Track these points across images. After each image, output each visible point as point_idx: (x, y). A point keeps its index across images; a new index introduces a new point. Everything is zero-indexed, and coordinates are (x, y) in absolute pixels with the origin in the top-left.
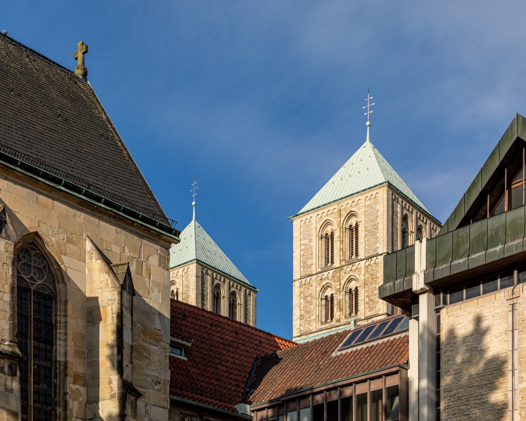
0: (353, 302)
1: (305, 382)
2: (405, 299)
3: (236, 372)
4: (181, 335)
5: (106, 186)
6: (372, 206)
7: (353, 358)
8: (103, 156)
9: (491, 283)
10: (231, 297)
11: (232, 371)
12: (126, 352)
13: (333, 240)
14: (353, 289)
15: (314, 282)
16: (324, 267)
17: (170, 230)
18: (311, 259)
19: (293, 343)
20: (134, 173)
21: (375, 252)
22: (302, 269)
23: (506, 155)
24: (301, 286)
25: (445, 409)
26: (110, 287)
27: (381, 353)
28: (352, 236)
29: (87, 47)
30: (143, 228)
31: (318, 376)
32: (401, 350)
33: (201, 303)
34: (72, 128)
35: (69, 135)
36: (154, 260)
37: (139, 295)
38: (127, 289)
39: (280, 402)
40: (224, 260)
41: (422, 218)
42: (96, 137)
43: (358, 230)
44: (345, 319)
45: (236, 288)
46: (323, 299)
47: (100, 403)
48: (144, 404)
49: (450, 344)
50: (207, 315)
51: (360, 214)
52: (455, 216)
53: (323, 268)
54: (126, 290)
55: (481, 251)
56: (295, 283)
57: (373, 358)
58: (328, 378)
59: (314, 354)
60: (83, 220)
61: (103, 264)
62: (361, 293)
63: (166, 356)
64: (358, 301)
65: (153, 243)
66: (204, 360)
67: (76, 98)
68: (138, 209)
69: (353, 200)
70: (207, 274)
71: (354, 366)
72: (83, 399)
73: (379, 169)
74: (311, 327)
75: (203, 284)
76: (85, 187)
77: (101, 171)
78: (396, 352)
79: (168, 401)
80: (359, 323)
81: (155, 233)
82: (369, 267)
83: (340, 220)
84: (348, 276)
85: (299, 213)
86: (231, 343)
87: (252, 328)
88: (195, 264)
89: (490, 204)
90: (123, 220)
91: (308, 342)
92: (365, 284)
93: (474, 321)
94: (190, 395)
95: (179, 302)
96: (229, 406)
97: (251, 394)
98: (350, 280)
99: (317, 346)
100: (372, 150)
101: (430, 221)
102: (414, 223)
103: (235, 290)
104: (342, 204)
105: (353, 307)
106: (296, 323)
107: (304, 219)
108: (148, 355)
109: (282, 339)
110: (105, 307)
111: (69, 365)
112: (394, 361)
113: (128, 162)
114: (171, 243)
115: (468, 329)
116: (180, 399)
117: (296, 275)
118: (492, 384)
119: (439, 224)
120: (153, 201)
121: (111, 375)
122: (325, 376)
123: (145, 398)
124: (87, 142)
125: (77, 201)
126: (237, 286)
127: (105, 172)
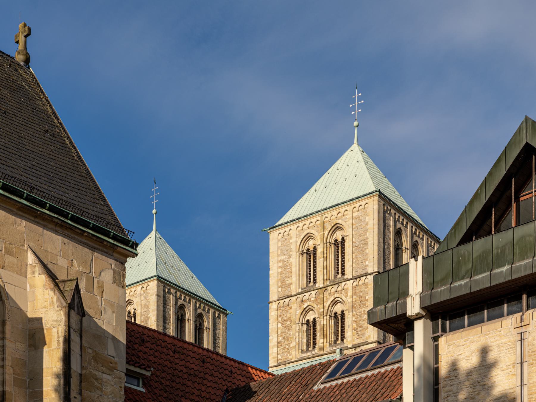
0: (338, 328)
2: (398, 325)
4: (139, 363)
5: (51, 189)
6: (361, 218)
7: (338, 392)
8: (48, 155)
9: (497, 308)
10: (198, 319)
12: (74, 381)
13: (316, 256)
14: (339, 313)
15: (294, 304)
16: (305, 287)
17: (126, 242)
18: (291, 278)
19: (269, 374)
20: (84, 175)
21: (363, 271)
22: (280, 289)
23: (513, 162)
24: (278, 308)
27: (370, 387)
28: (338, 252)
29: (29, 29)
30: (95, 238)
32: (394, 384)
33: (162, 326)
34: (12, 122)
35: (8, 130)
36: (107, 276)
37: (90, 316)
38: (76, 308)
40: (189, 277)
41: (417, 233)
42: (40, 133)
43: (344, 245)
44: (329, 347)
45: (204, 310)
46: (304, 324)
49: (449, 377)
51: (346, 227)
52: (455, 231)
53: (304, 288)
54: (74, 310)
55: (485, 272)
56: (272, 305)
57: (362, 392)
59: (293, 387)
60: (24, 229)
61: (48, 279)
62: (348, 318)
63: (121, 387)
64: (344, 327)
65: (106, 256)
66: (165, 392)
67: (17, 87)
68: (89, 216)
69: (338, 211)
70: (170, 293)
73: (369, 176)
74: (290, 355)
76: (27, 190)
77: (45, 172)
78: (388, 386)
80: (345, 352)
81: (109, 244)
82: (357, 288)
83: (324, 234)
84: (332, 298)
85: (277, 224)
86: (197, 373)
87: (221, 356)
90: (71, 229)
91: (286, 373)
92: (352, 307)
98: (335, 302)
99: (297, 377)
100: (360, 154)
101: (427, 237)
102: (408, 239)
103: (202, 312)
104: (326, 215)
105: (338, 333)
106: (273, 351)
107: (282, 231)
108: (100, 385)
109: (256, 370)
110: (49, 329)
111: (7, 396)
112: (385, 396)
113: (77, 162)
114: (127, 256)
117: (273, 296)
120: (106, 208)
125: (17, 207)
126: (204, 307)
127: (50, 173)
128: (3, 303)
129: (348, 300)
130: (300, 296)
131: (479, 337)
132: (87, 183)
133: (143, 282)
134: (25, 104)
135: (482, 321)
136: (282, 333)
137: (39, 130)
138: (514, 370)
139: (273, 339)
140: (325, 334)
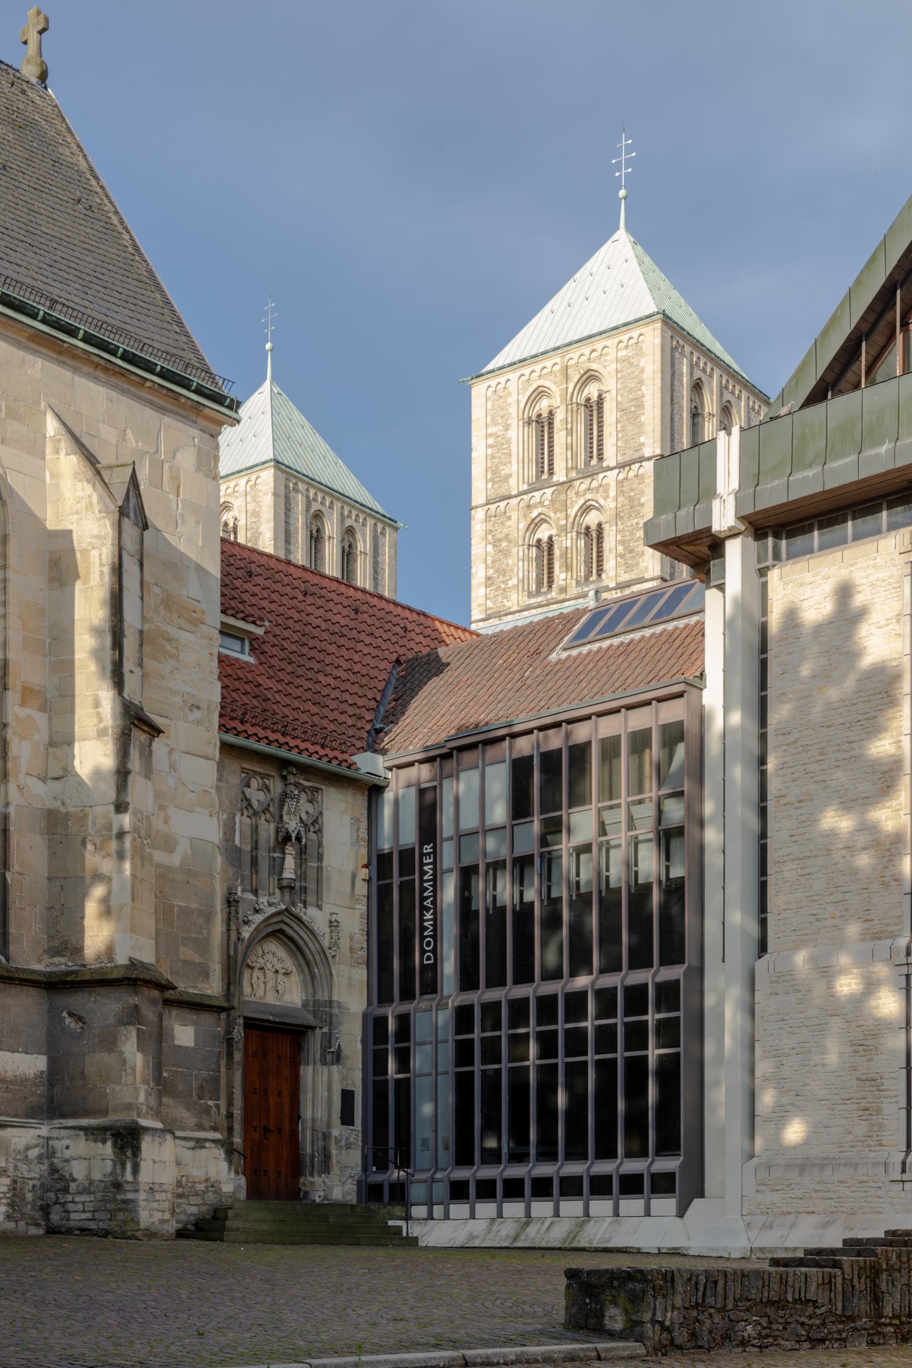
1: (495, 711)
2: (698, 547)
3: (355, 688)
4: (242, 612)
5: (87, 304)
6: (632, 361)
9: (869, 518)
10: (346, 537)
11: (347, 686)
12: (130, 643)
13: (553, 428)
14: (594, 527)
15: (514, 511)
17: (218, 399)
19: (471, 633)
20: (145, 279)
22: (490, 485)
23: (899, 261)
24: (488, 518)
25: (781, 767)
26: (96, 511)
28: (591, 420)
29: (47, 20)
30: (165, 392)
31: (522, 700)
32: (691, 651)
34: (17, 184)
35: (10, 197)
36: (187, 459)
37: (157, 529)
38: (132, 515)
39: (444, 751)
42: (67, 205)
43: (602, 408)
45: (356, 521)
47: (77, 746)
48: (167, 749)
49: (786, 639)
50: (297, 573)
52: (797, 382)
53: (533, 484)
54: (128, 517)
55: (850, 454)
57: (633, 666)
58: (543, 703)
59: (514, 656)
60: (39, 373)
61: (82, 463)
62: (609, 535)
63: (211, 654)
64: (602, 551)
65: (185, 424)
66: (289, 663)
67: (25, 122)
68: (155, 353)
71: (594, 681)
72: (42, 736)
73: (645, 287)
75: (288, 510)
76: (44, 306)
77: (77, 273)
78: (679, 654)
79: (215, 744)
80: (605, 595)
81: (189, 403)
82: (625, 484)
84: (581, 501)
85: (484, 370)
86: (345, 631)
87: (388, 601)
88: (272, 470)
89: (867, 360)
90: (123, 375)
91: (502, 631)
92: (618, 517)
93: (836, 595)
94: (262, 733)
95: (239, 545)
96: (341, 757)
97: (386, 734)
98: (586, 509)
99: (520, 639)
101: (747, 394)
103: (355, 525)
106: (478, 593)
107: (493, 383)
108: (174, 651)
109: (449, 625)
110: (85, 552)
111: (12, 668)
113: (132, 257)
114: (220, 424)
115: (823, 610)
116: (240, 741)
117: (478, 496)
118: (870, 721)
119: (766, 401)
120: (184, 339)
121: (98, 690)
122: (537, 700)
123: (169, 737)
124: (48, 213)
125: (26, 334)
126: (357, 516)
127: (84, 276)
128: (4, 504)
129: (610, 504)
130: (525, 497)
131: (838, 569)
132: (150, 293)
133: (249, 471)
134: (40, 152)
135: (844, 541)
136: (493, 562)
137: (66, 199)
138: (898, 627)
139: (478, 573)
140: (569, 563)
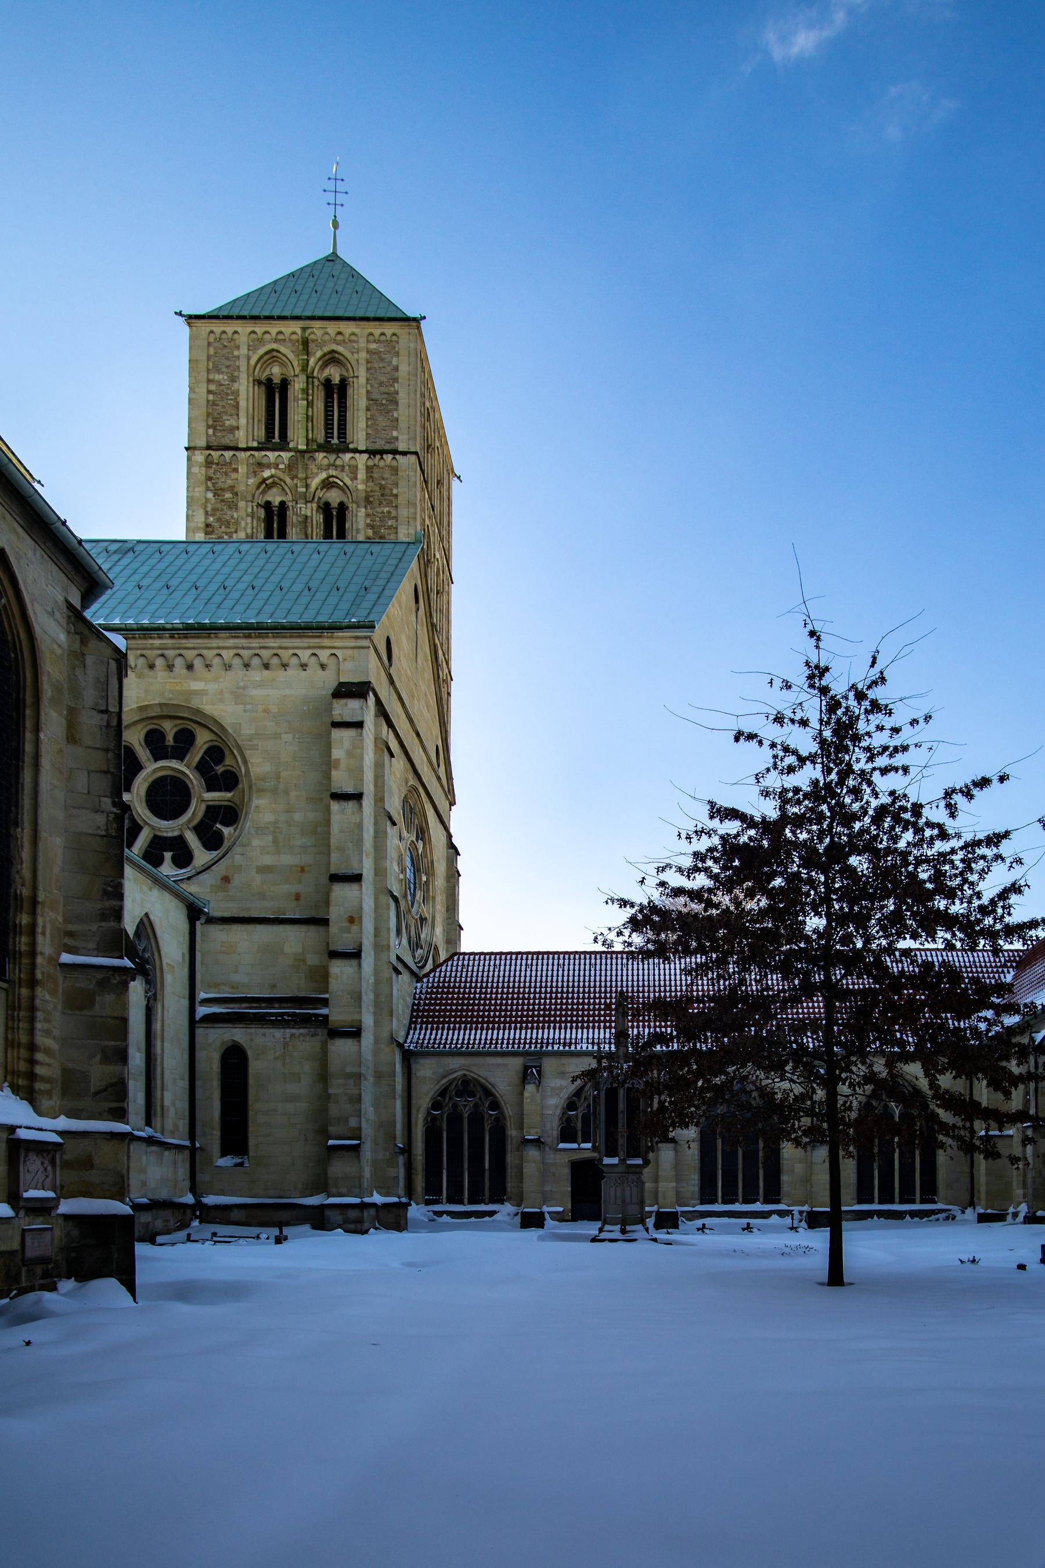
22: (211, 431)
